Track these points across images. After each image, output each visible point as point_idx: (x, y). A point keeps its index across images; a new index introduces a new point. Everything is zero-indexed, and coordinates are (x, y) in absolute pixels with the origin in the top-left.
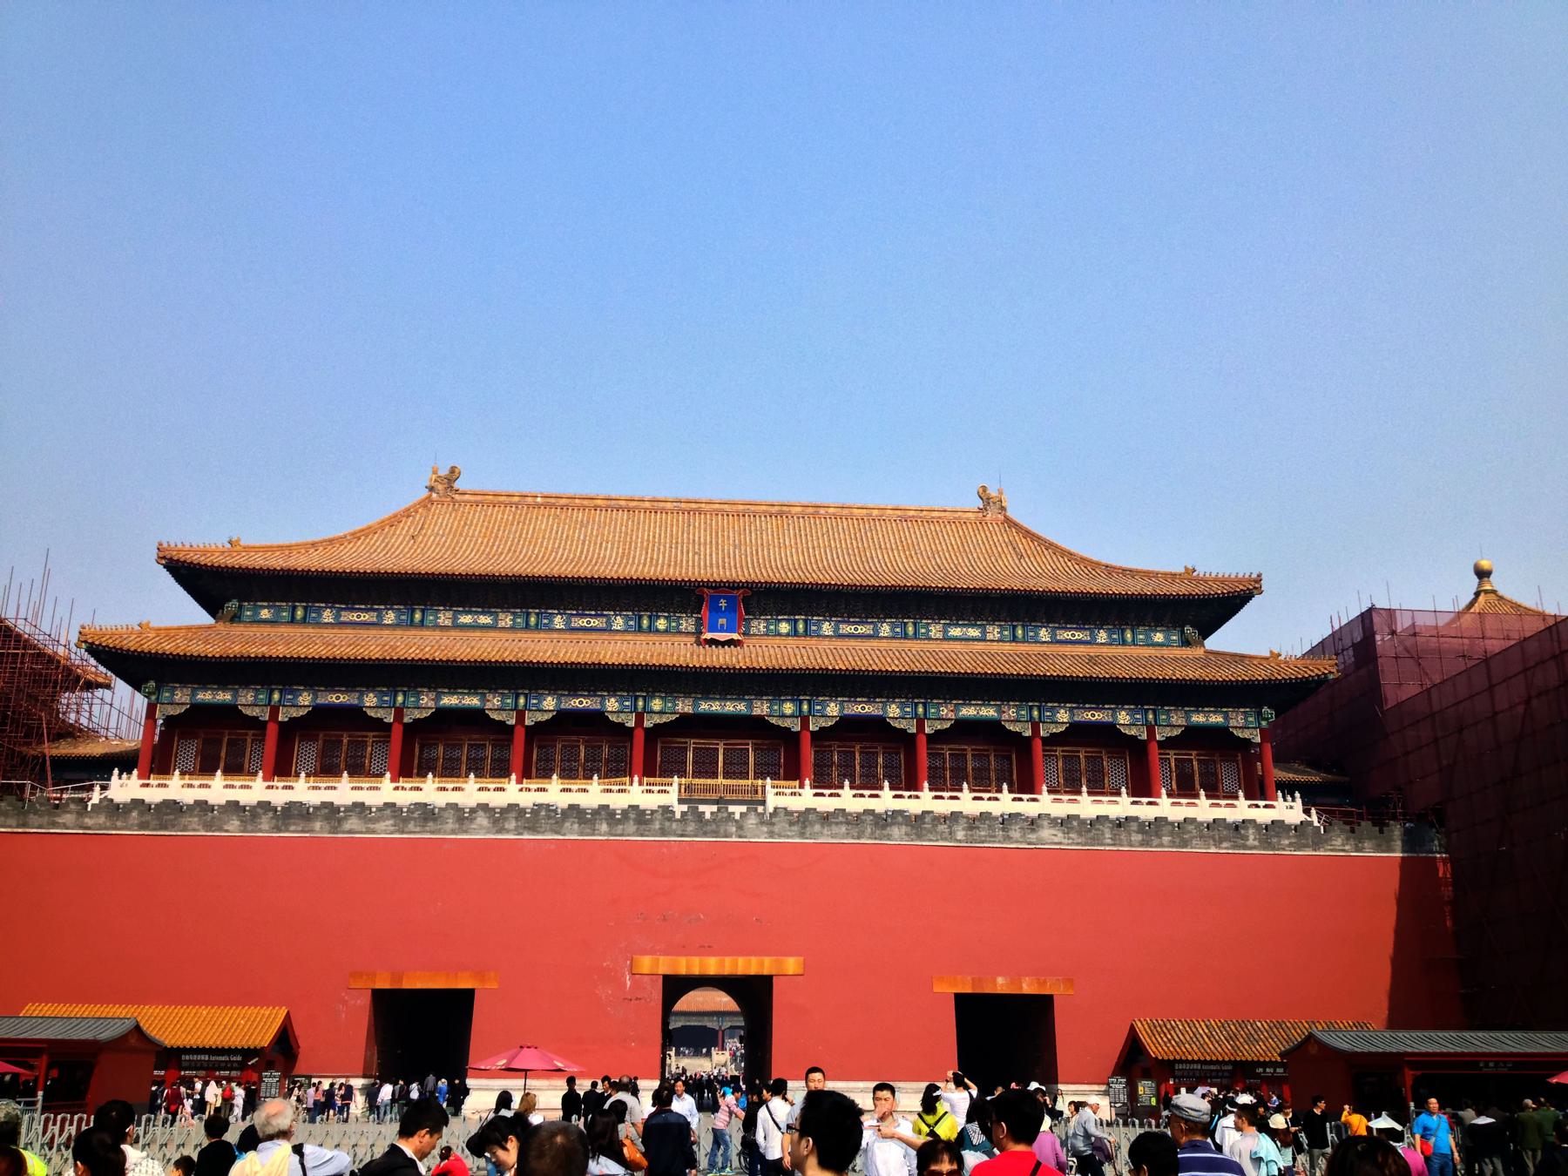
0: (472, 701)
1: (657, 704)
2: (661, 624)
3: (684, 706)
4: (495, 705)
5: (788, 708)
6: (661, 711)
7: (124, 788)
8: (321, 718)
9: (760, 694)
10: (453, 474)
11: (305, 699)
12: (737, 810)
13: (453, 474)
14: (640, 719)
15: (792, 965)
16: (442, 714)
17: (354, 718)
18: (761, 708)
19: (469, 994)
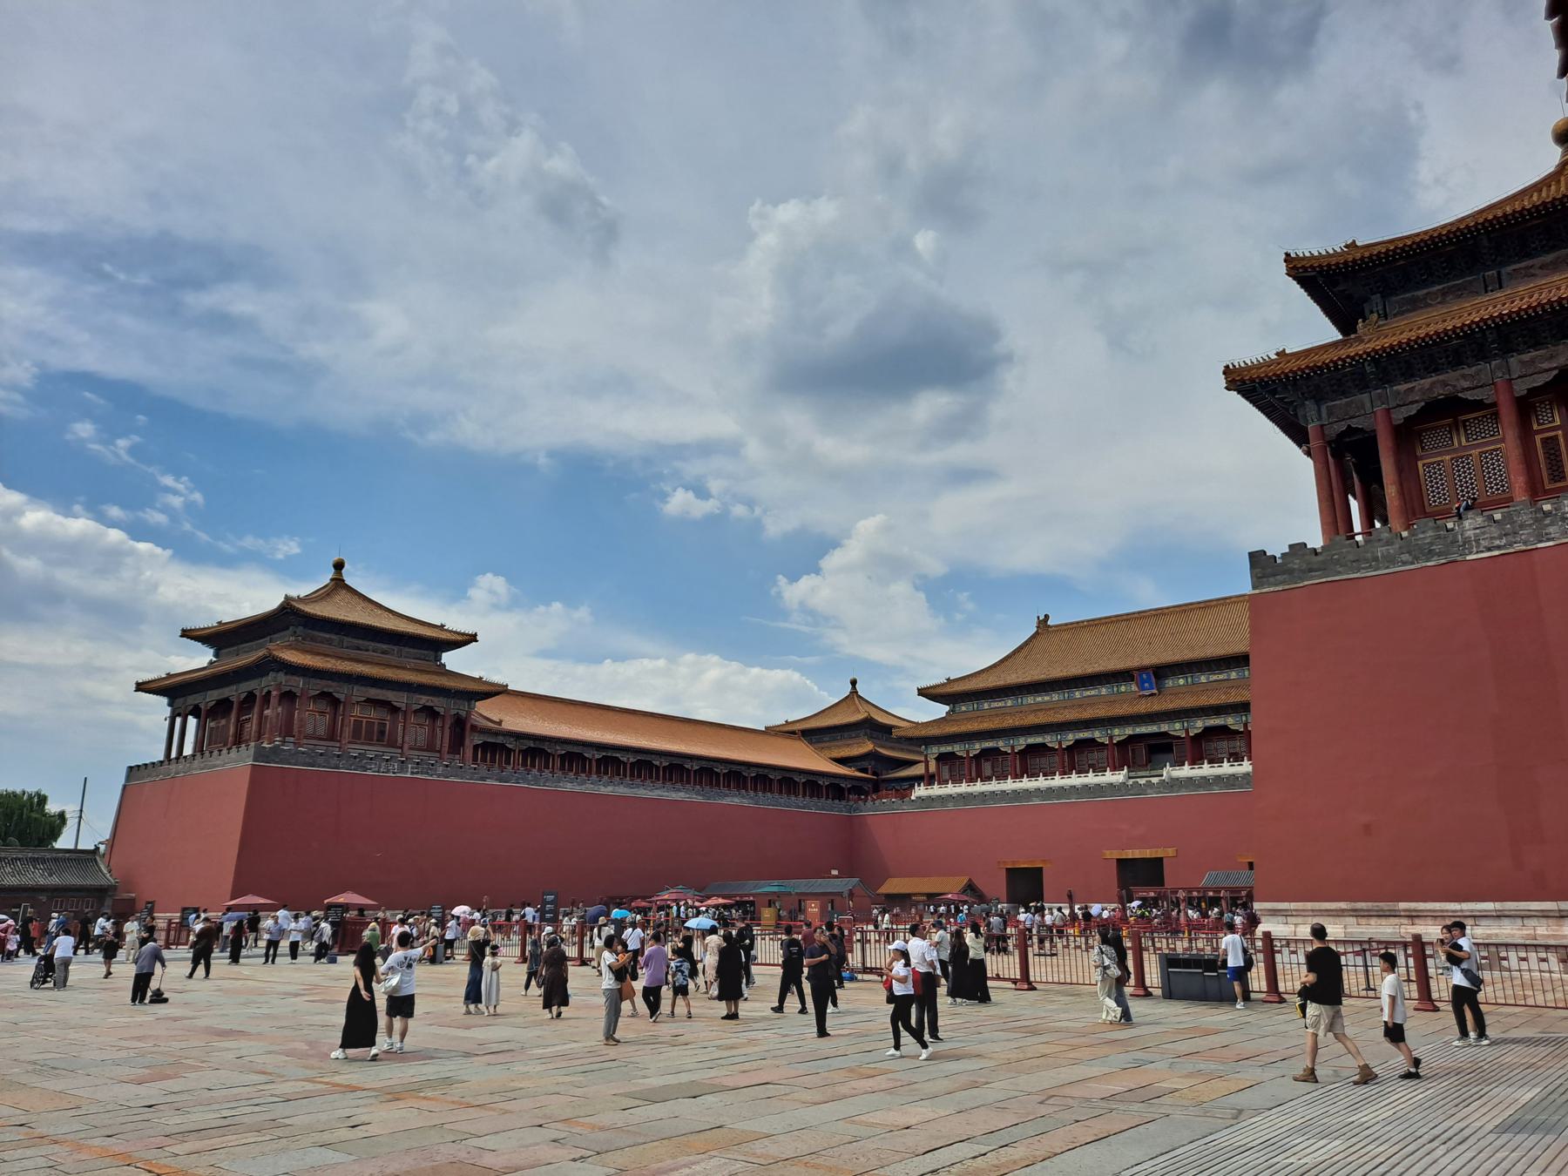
0: (1039, 740)
1: (1116, 732)
2: (1123, 689)
3: (1129, 731)
4: (1049, 740)
5: (1178, 726)
6: (1120, 733)
7: (920, 791)
8: (985, 753)
9: (1163, 721)
10: (1047, 617)
11: (977, 746)
12: (1142, 781)
13: (1047, 617)
14: (1111, 738)
15: (1171, 852)
16: (1029, 746)
17: (996, 751)
18: (1164, 728)
19: (1041, 869)
